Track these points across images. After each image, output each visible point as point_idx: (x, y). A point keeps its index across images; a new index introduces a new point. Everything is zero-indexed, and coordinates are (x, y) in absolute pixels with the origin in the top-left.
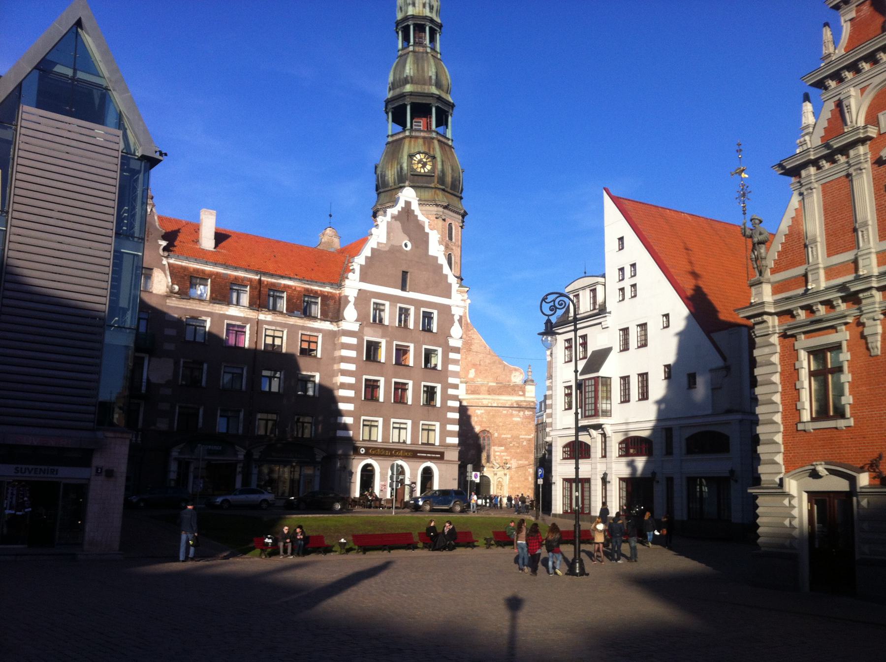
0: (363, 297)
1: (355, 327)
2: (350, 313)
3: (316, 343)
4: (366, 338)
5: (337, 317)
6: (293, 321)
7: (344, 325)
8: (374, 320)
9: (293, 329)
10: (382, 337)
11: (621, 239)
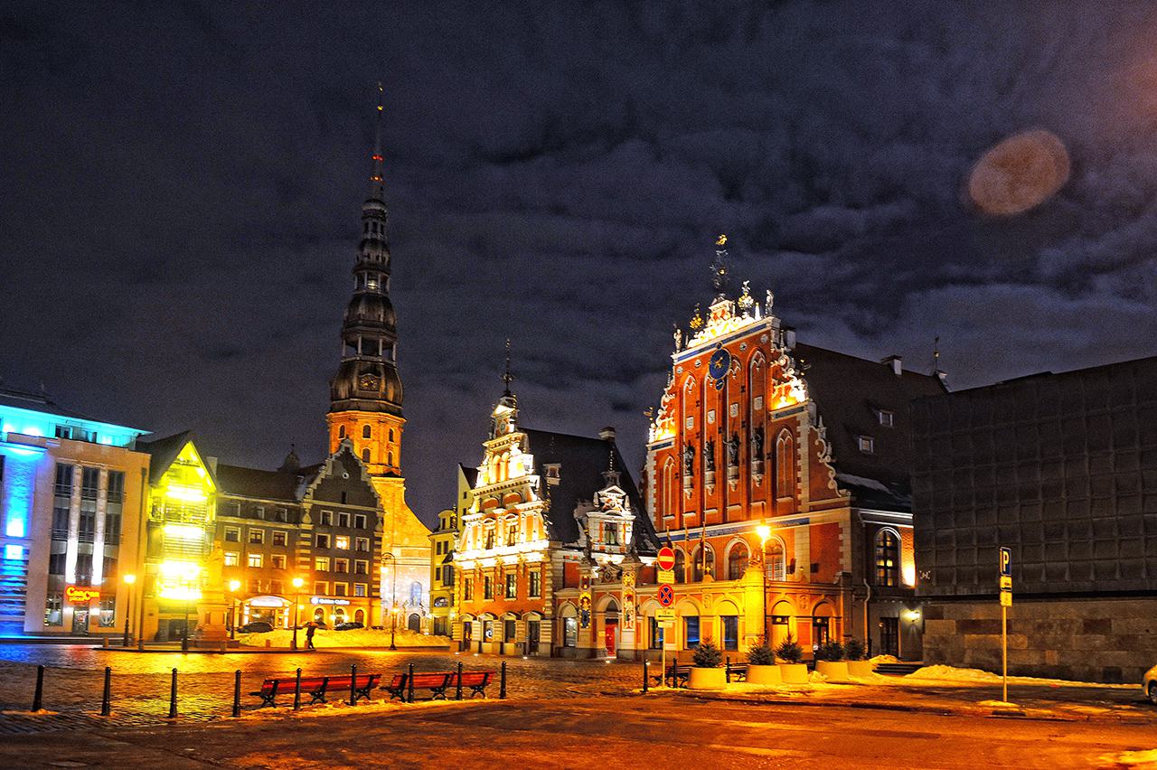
0: (315, 509)
1: (310, 527)
2: (306, 518)
3: (284, 537)
4: (317, 534)
5: (298, 522)
6: (268, 524)
7: (303, 526)
8: (323, 523)
9: (268, 530)
10: (328, 533)
11: (465, 493)
